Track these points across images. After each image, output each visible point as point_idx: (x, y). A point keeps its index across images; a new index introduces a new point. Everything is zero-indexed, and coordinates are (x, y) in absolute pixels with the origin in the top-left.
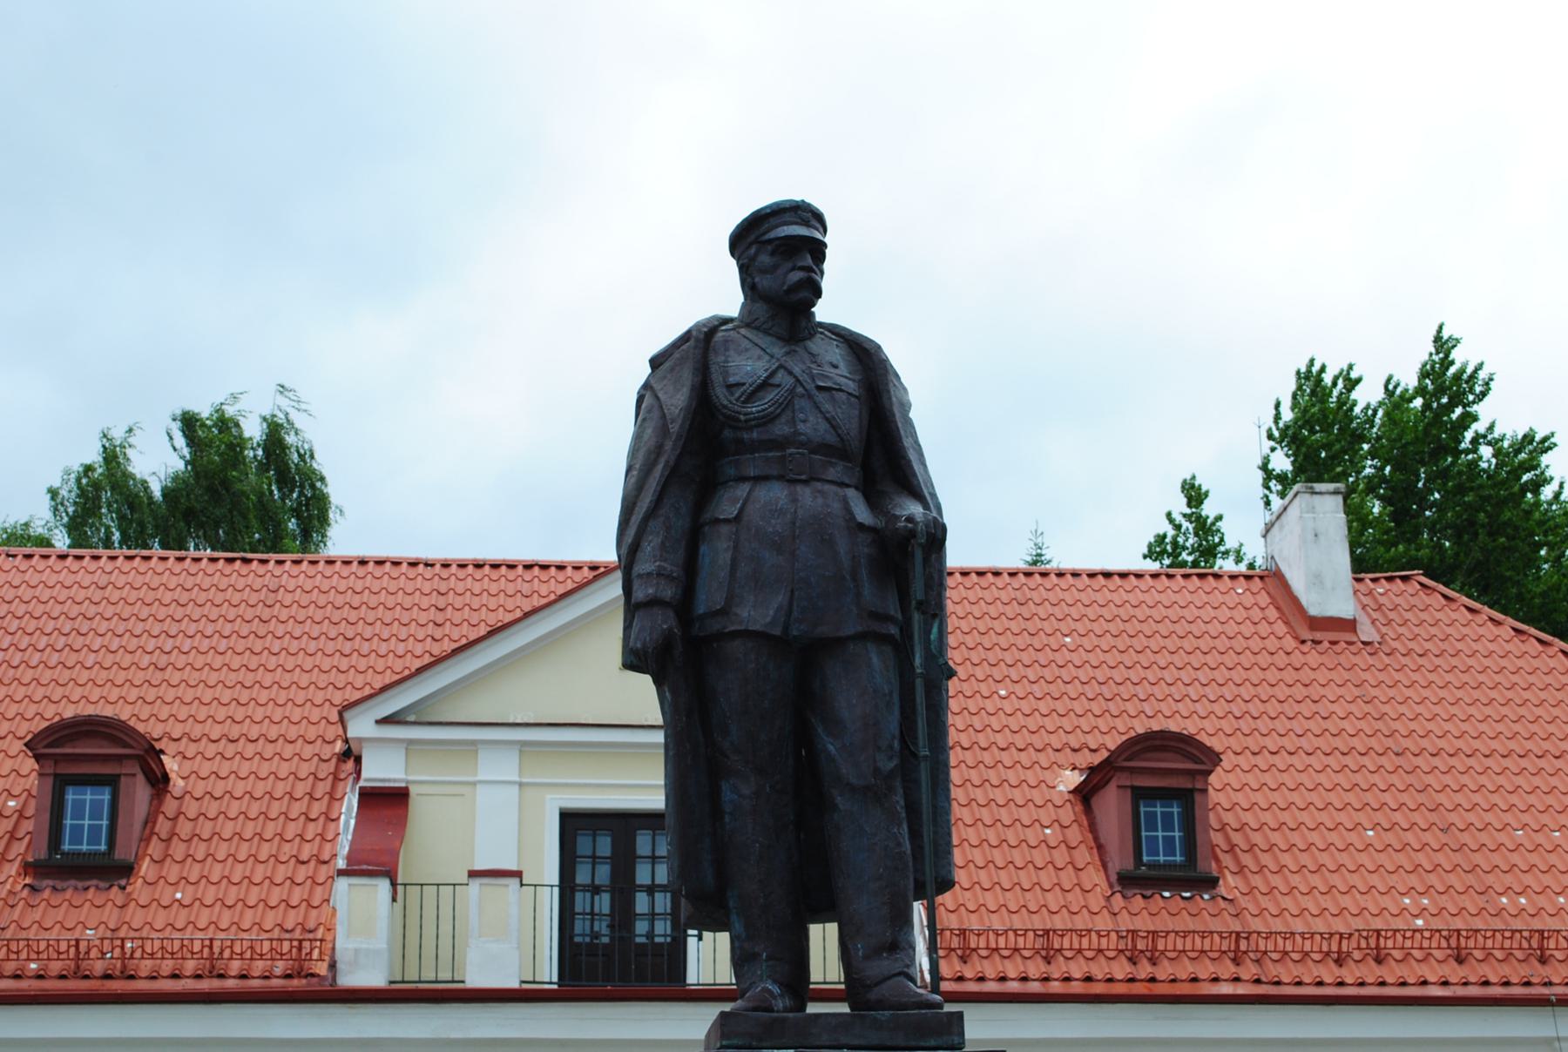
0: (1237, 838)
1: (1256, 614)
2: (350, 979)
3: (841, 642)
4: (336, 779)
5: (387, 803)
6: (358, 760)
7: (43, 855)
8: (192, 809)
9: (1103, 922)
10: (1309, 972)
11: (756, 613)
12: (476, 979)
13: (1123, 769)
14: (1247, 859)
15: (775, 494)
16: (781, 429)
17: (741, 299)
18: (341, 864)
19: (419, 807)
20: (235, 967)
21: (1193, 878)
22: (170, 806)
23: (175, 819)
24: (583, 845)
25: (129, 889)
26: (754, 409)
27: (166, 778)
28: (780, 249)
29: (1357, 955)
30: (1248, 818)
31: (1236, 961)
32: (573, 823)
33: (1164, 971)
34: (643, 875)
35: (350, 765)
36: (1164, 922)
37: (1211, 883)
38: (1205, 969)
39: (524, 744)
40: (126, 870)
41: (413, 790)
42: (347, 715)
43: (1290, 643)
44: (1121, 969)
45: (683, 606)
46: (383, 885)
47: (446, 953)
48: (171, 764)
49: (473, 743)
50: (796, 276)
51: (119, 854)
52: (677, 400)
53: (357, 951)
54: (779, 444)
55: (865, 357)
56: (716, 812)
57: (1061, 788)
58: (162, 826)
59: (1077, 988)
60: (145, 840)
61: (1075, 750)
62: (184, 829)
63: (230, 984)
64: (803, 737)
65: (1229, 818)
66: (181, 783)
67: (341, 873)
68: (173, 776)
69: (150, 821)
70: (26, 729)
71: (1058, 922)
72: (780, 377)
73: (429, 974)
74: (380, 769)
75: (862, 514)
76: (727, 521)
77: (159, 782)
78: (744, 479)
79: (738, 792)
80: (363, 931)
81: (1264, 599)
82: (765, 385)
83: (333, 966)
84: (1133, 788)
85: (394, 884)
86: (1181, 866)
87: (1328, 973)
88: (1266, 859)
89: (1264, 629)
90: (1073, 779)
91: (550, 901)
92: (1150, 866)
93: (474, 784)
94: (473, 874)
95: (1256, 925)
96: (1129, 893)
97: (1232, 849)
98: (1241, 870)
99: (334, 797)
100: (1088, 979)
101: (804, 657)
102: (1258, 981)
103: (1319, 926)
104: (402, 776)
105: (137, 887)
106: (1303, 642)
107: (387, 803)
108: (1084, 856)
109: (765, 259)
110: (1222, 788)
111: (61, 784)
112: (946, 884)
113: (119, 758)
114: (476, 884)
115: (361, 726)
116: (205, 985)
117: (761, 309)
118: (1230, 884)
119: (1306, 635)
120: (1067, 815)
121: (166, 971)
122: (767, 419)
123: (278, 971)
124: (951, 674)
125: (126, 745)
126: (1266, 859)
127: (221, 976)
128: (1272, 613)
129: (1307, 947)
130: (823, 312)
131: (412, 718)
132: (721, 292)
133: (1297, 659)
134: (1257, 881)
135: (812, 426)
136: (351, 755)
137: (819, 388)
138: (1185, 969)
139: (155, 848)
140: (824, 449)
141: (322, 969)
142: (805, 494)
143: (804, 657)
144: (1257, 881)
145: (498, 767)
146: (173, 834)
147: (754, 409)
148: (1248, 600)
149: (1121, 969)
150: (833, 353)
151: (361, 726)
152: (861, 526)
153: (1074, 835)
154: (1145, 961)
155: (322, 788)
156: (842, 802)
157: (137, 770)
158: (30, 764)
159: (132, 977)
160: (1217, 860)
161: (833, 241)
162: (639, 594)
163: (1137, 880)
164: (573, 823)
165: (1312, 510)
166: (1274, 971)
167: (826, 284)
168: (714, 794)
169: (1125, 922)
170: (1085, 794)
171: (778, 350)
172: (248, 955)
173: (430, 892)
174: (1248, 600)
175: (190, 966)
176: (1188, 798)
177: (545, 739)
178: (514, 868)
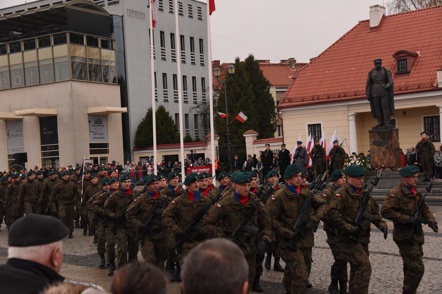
7: (397, 72)
11: (375, 95)
15: (376, 85)
22: (417, 60)
27: (417, 55)
40: (409, 72)
45: (370, 95)
51: (409, 70)
58: (416, 63)
60: (412, 66)
70: (393, 53)
79: (376, 109)
83: (437, 84)
101: (380, 98)
111: (398, 61)
122: (375, 79)
135: (379, 79)
143: (380, 98)
146: (417, 65)
158: (394, 59)
171: (377, 72)
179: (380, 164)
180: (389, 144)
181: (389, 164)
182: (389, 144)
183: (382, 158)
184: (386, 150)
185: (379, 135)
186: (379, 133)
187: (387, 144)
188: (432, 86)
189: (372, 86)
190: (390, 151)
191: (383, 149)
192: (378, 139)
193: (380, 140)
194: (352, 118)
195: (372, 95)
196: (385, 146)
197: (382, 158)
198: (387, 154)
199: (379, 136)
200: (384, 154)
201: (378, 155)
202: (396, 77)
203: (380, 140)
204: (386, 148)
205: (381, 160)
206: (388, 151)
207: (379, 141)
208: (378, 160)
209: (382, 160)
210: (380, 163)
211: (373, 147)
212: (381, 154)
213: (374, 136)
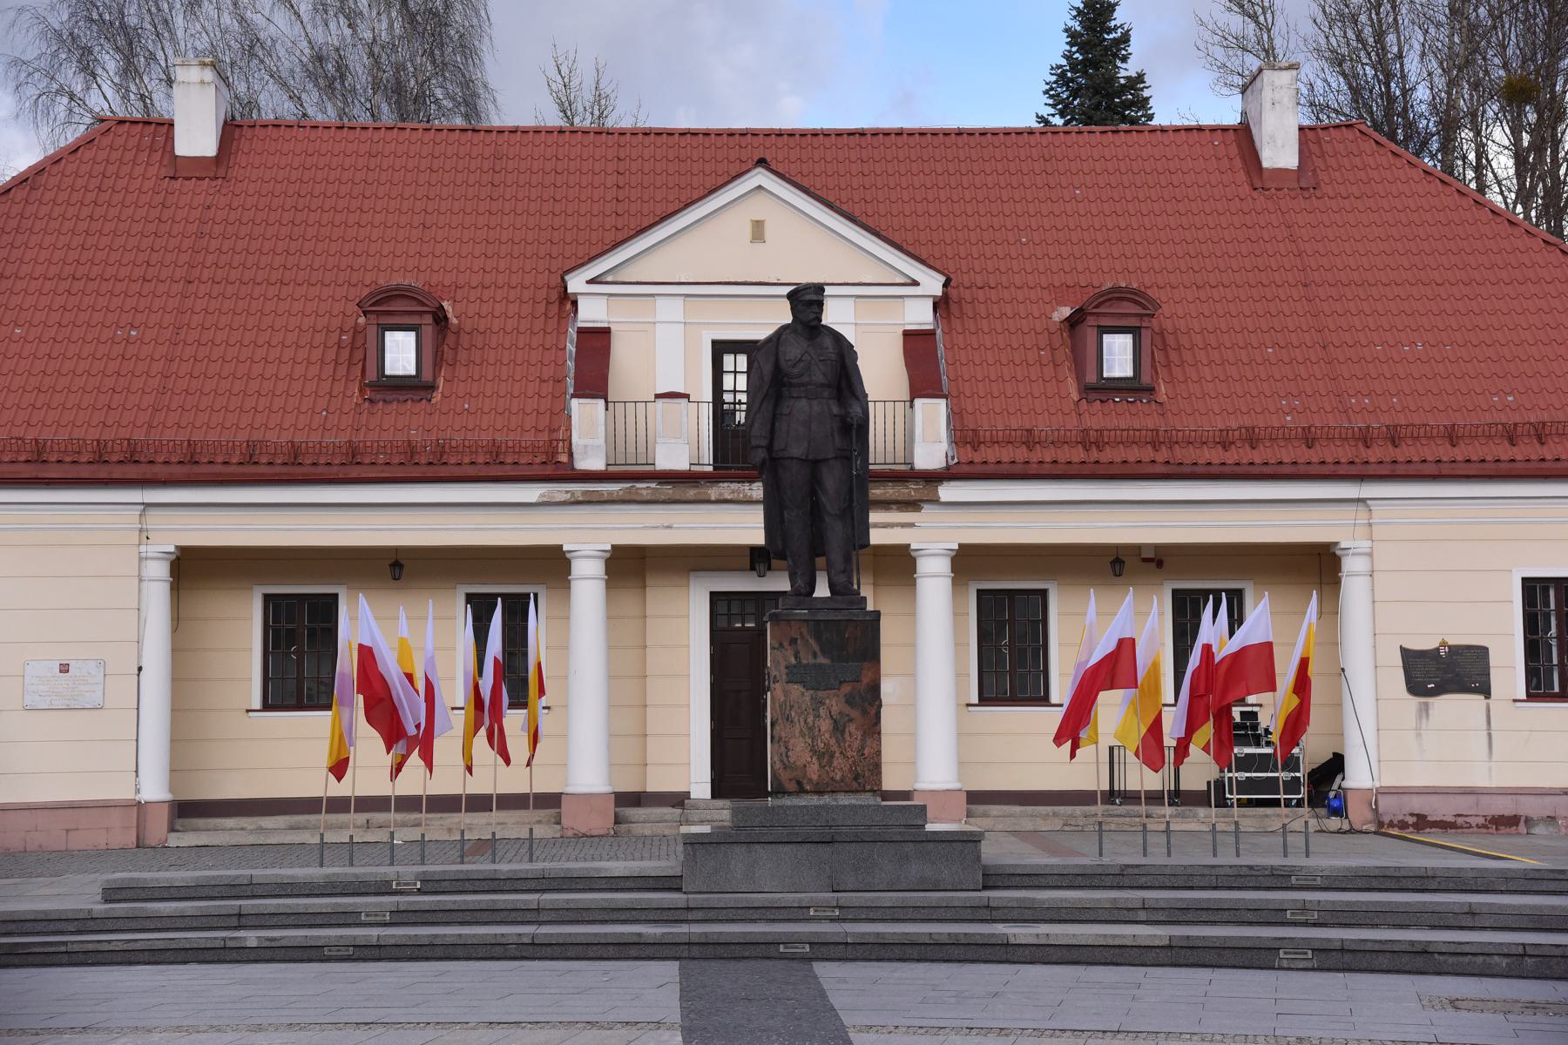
3: (825, 460)
5: (597, 341)
6: (575, 303)
9: (1072, 422)
11: (797, 451)
15: (803, 402)
16: (805, 379)
18: (571, 390)
22: (450, 339)
23: (455, 349)
24: (728, 360)
26: (795, 371)
27: (446, 318)
35: (569, 306)
37: (1151, 390)
40: (432, 387)
43: (1247, 188)
46: (601, 402)
47: (641, 449)
50: (812, 316)
54: (803, 385)
55: (838, 338)
56: (782, 522)
58: (448, 354)
59: (1047, 469)
64: (813, 492)
66: (455, 321)
67: (573, 396)
68: (450, 315)
72: (806, 357)
74: (591, 312)
75: (835, 410)
80: (589, 432)
81: (1234, 150)
83: (571, 455)
85: (607, 402)
90: (1066, 311)
91: (707, 412)
94: (658, 396)
96: (1092, 396)
104: (604, 317)
107: (597, 341)
109: (800, 307)
113: (421, 313)
114: (660, 401)
117: (799, 327)
121: (467, 460)
125: (424, 304)
128: (1238, 163)
131: (609, 279)
136: (569, 302)
140: (822, 385)
141: (564, 458)
142: (815, 402)
143: (814, 465)
145: (670, 310)
147: (795, 371)
150: (828, 342)
151: (576, 283)
153: (1063, 353)
154: (1094, 448)
155: (552, 324)
156: (827, 519)
164: (721, 349)
166: (1180, 454)
168: (782, 514)
170: (1074, 322)
173: (630, 406)
179: (815, 777)
180: (865, 680)
181: (856, 779)
182: (865, 680)
183: (827, 745)
184: (847, 709)
185: (818, 636)
186: (818, 629)
187: (857, 681)
189: (776, 405)
190: (865, 712)
191: (835, 703)
192: (812, 655)
193: (822, 660)
194: (159, 570)
195: (778, 445)
196: (846, 689)
197: (827, 745)
198: (852, 727)
199: (818, 637)
200: (838, 728)
201: (811, 729)
202: (371, 401)
203: (822, 660)
204: (850, 700)
205: (820, 756)
206: (855, 714)
207: (821, 665)
208: (807, 757)
209: (825, 756)
211: (786, 693)
212: (825, 725)
213: (793, 641)
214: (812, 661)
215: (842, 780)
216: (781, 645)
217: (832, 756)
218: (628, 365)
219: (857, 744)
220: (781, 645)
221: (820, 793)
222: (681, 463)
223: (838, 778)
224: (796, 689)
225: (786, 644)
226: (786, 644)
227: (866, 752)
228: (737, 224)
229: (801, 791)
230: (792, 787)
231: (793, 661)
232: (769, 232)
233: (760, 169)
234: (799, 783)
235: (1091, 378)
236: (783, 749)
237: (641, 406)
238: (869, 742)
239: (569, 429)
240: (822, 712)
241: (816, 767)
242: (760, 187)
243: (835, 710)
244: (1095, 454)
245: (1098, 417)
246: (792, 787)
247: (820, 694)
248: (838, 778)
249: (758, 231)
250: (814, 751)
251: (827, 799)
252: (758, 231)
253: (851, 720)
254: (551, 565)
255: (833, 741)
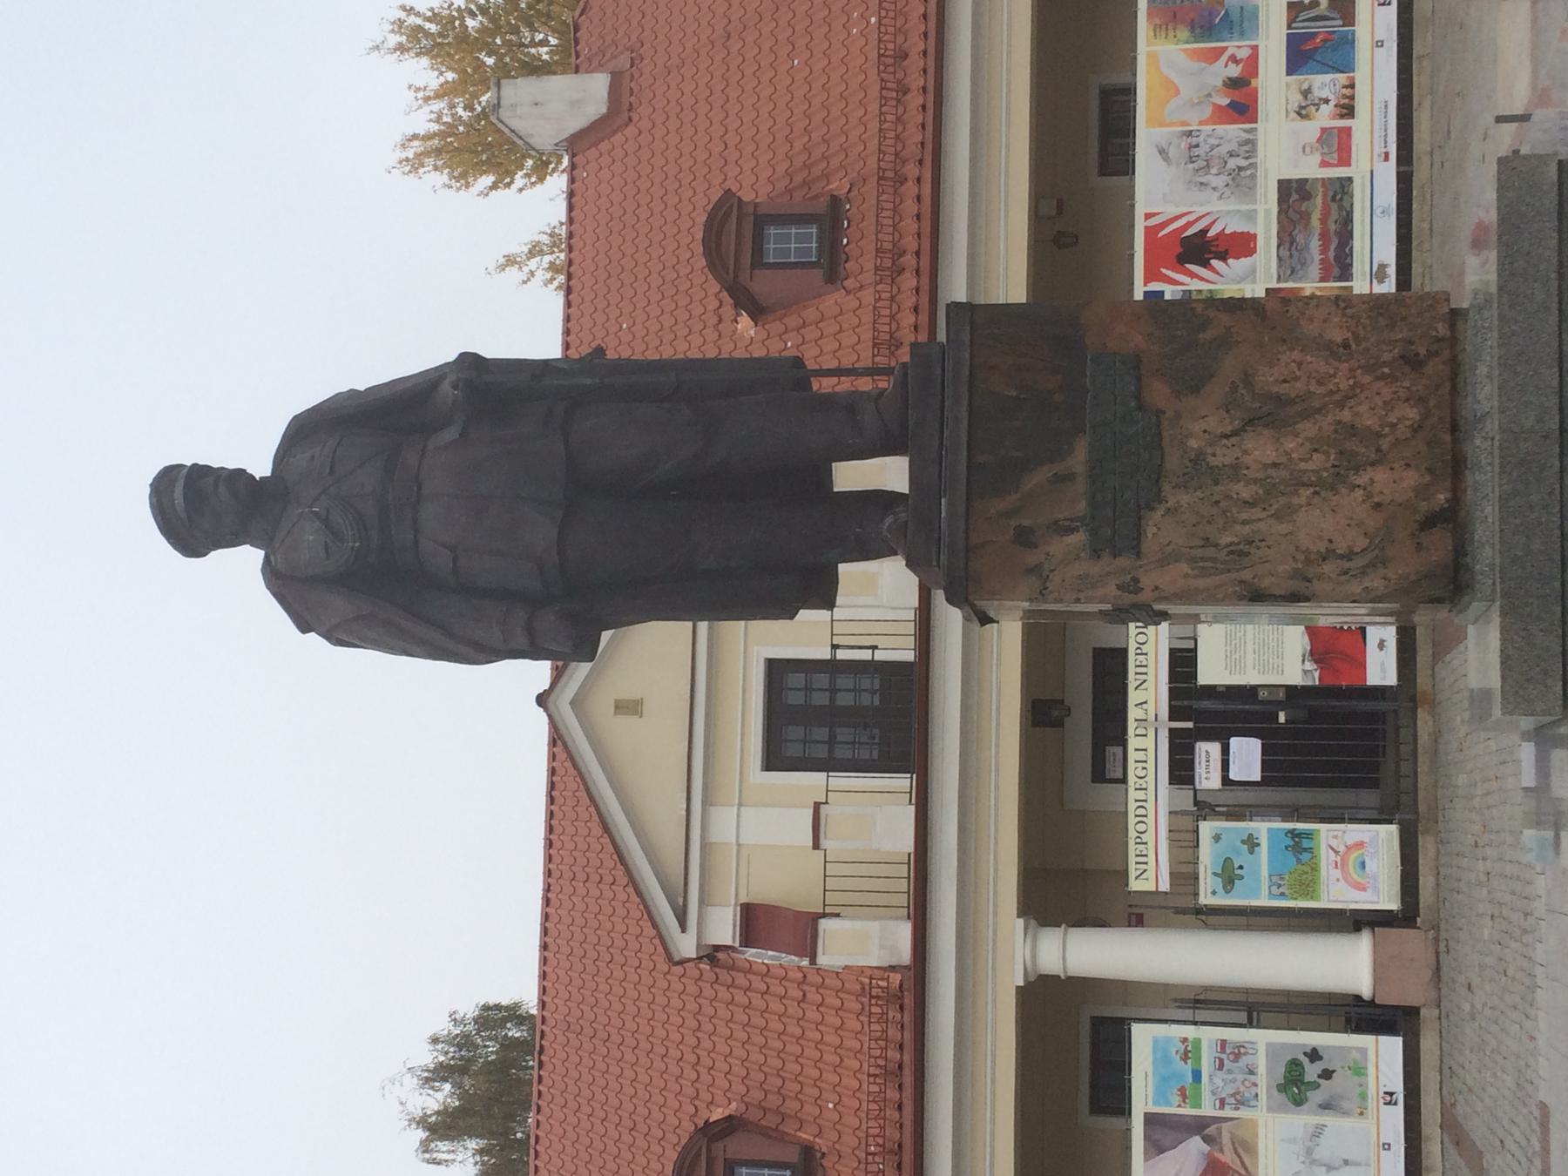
0: (798, 179)
1: (605, 160)
2: (905, 954)
4: (732, 967)
6: (717, 948)
8: (757, 1095)
9: (868, 296)
10: (914, 117)
12: (907, 844)
13: (736, 276)
14: (817, 171)
17: (248, 547)
18: (805, 962)
19: (757, 897)
20: (893, 1054)
21: (831, 219)
22: (754, 1115)
24: (794, 750)
25: (824, 1150)
27: (730, 1117)
28: (197, 508)
29: (900, 75)
30: (781, 169)
31: (904, 181)
32: (775, 759)
33: (910, 243)
34: (821, 699)
35: (720, 955)
36: (869, 245)
37: (835, 202)
38: (910, 207)
39: (707, 802)
40: (808, 1151)
41: (743, 900)
42: (677, 958)
43: (630, 131)
44: (908, 281)
46: (824, 924)
48: (717, 1114)
49: (705, 846)
50: (222, 489)
51: (793, 1155)
52: (340, 605)
53: (882, 947)
57: (752, 332)
58: (771, 1121)
61: (720, 321)
62: (773, 1101)
63: (908, 1058)
65: (780, 186)
66: (734, 1105)
67: (813, 961)
68: (727, 1113)
69: (765, 1132)
71: (867, 336)
73: (900, 886)
74: (723, 928)
75: (450, 434)
76: (455, 560)
77: (731, 1125)
78: (416, 542)
80: (863, 942)
82: (326, 522)
83: (893, 968)
84: (753, 267)
85: (824, 915)
86: (820, 229)
87: (914, 100)
88: (816, 154)
89: (619, 153)
90: (745, 322)
91: (841, 780)
92: (819, 256)
93: (739, 845)
94: (816, 845)
95: (872, 162)
96: (843, 274)
97: (806, 184)
98: (826, 176)
99: (749, 969)
100: (916, 309)
102: (921, 162)
103: (874, 107)
105: (821, 1144)
106: (630, 119)
108: (810, 314)
110: (754, 189)
112: (798, 362)
114: (824, 843)
115: (686, 946)
116: (908, 1079)
118: (838, 186)
119: (626, 115)
120: (776, 327)
123: (899, 1016)
124: (600, 351)
125: (698, 1154)
126: (816, 154)
127: (900, 1066)
128: (605, 146)
129: (893, 118)
130: (261, 467)
132: (242, 565)
133: (645, 124)
134: (835, 162)
136: (712, 955)
137: (332, 468)
138: (909, 225)
139: (789, 1128)
141: (896, 978)
144: (835, 162)
145: (724, 824)
148: (593, 166)
149: (908, 281)
151: (686, 946)
152: (464, 433)
153: (792, 321)
155: (741, 980)
157: (720, 1145)
159: (900, 1146)
160: (816, 197)
161: (187, 458)
162: (521, 641)
163: (832, 265)
164: (775, 759)
165: (514, 106)
166: (912, 149)
167: (231, 464)
169: (868, 277)
170: (758, 313)
172: (882, 1043)
173: (831, 883)
174: (593, 166)
175: (892, 1094)
176: (762, 220)
177: (702, 784)
178: (811, 811)
179: (1412, 478)
181: (1413, 363)
187: (1136, 363)
188: (896, 998)
191: (1201, 425)
193: (1079, 457)
196: (1159, 392)
198: (1268, 378)
200: (1273, 414)
203: (1079, 457)
204: (1192, 383)
208: (1351, 502)
209: (1351, 454)
210: (1394, 482)
211: (1164, 562)
212: (1260, 449)
213: (1025, 538)
214: (1081, 485)
215: (1422, 400)
216: (1035, 570)
217: (1352, 430)
218: (787, 881)
219: (1318, 364)
220: (1035, 570)
221: (1457, 466)
222: (907, 815)
223: (1413, 414)
224: (1159, 530)
225: (1032, 558)
226: (1032, 558)
227: (1338, 336)
228: (621, 731)
229: (1451, 519)
230: (1439, 545)
231: (1078, 538)
232: (627, 692)
233: (550, 705)
234: (1429, 522)
235: (818, 275)
236: (1328, 568)
237: (831, 870)
238: (1312, 329)
239: (862, 970)
240: (1222, 457)
241: (1380, 476)
242: (572, 703)
243: (1216, 423)
244: (909, 260)
245: (862, 263)
246: (1439, 545)
247: (1173, 462)
248: (1413, 414)
249: (628, 707)
250: (1336, 480)
251: (1484, 448)
252: (628, 707)
253: (1247, 378)
254: (1045, 1000)
255: (1308, 429)
